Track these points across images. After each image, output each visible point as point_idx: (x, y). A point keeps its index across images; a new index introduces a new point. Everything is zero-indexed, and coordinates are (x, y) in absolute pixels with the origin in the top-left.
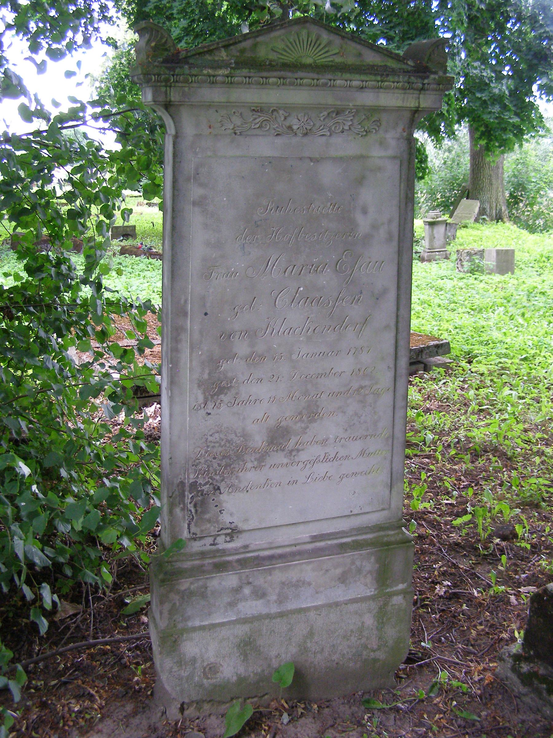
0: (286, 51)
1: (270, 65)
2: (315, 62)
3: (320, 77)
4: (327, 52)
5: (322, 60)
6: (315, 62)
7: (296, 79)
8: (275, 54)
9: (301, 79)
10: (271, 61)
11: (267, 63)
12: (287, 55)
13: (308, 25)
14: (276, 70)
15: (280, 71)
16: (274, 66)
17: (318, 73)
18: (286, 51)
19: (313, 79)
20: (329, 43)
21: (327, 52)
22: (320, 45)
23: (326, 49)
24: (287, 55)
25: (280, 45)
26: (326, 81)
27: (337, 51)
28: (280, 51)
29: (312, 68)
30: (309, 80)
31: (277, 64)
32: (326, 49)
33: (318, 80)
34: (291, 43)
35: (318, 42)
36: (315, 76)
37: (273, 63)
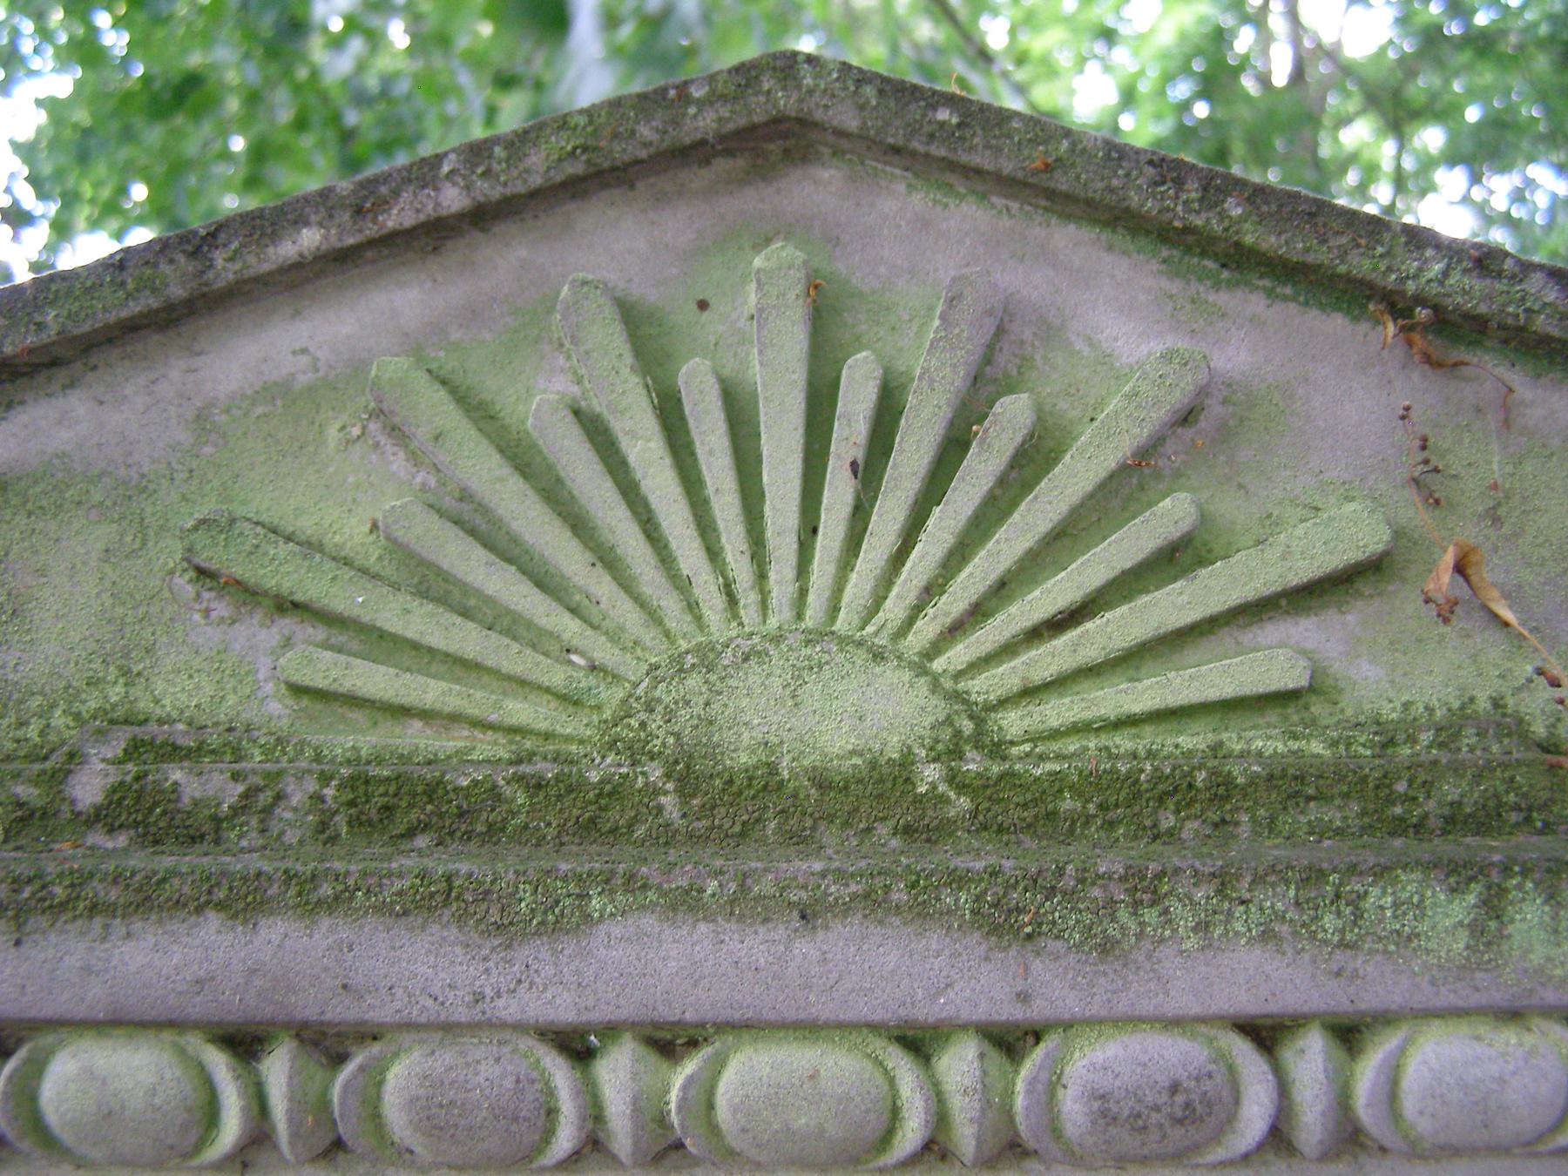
0: (434, 586)
1: (140, 811)
2: (969, 729)
3: (1053, 983)
4: (1175, 559)
5: (1072, 710)
6: (969, 729)
7: (577, 1047)
8: (259, 636)
9: (668, 1042)
10: (150, 748)
11: (89, 789)
12: (467, 639)
13: (819, 189)
14: (244, 902)
15: (309, 898)
16: (199, 830)
17: (1005, 922)
18: (434, 586)
19: (919, 1042)
20: (1197, 426)
21: (1175, 559)
22: (1033, 459)
23: (1170, 515)
24: (467, 639)
25: (349, 499)
26: (1174, 1054)
27: (1355, 532)
28: (352, 599)
29: (924, 828)
30: (838, 1067)
31: (259, 802)
32: (1170, 515)
33: (1008, 1042)
34: (524, 459)
35: (1012, 416)
36: (962, 976)
37: (200, 786)
